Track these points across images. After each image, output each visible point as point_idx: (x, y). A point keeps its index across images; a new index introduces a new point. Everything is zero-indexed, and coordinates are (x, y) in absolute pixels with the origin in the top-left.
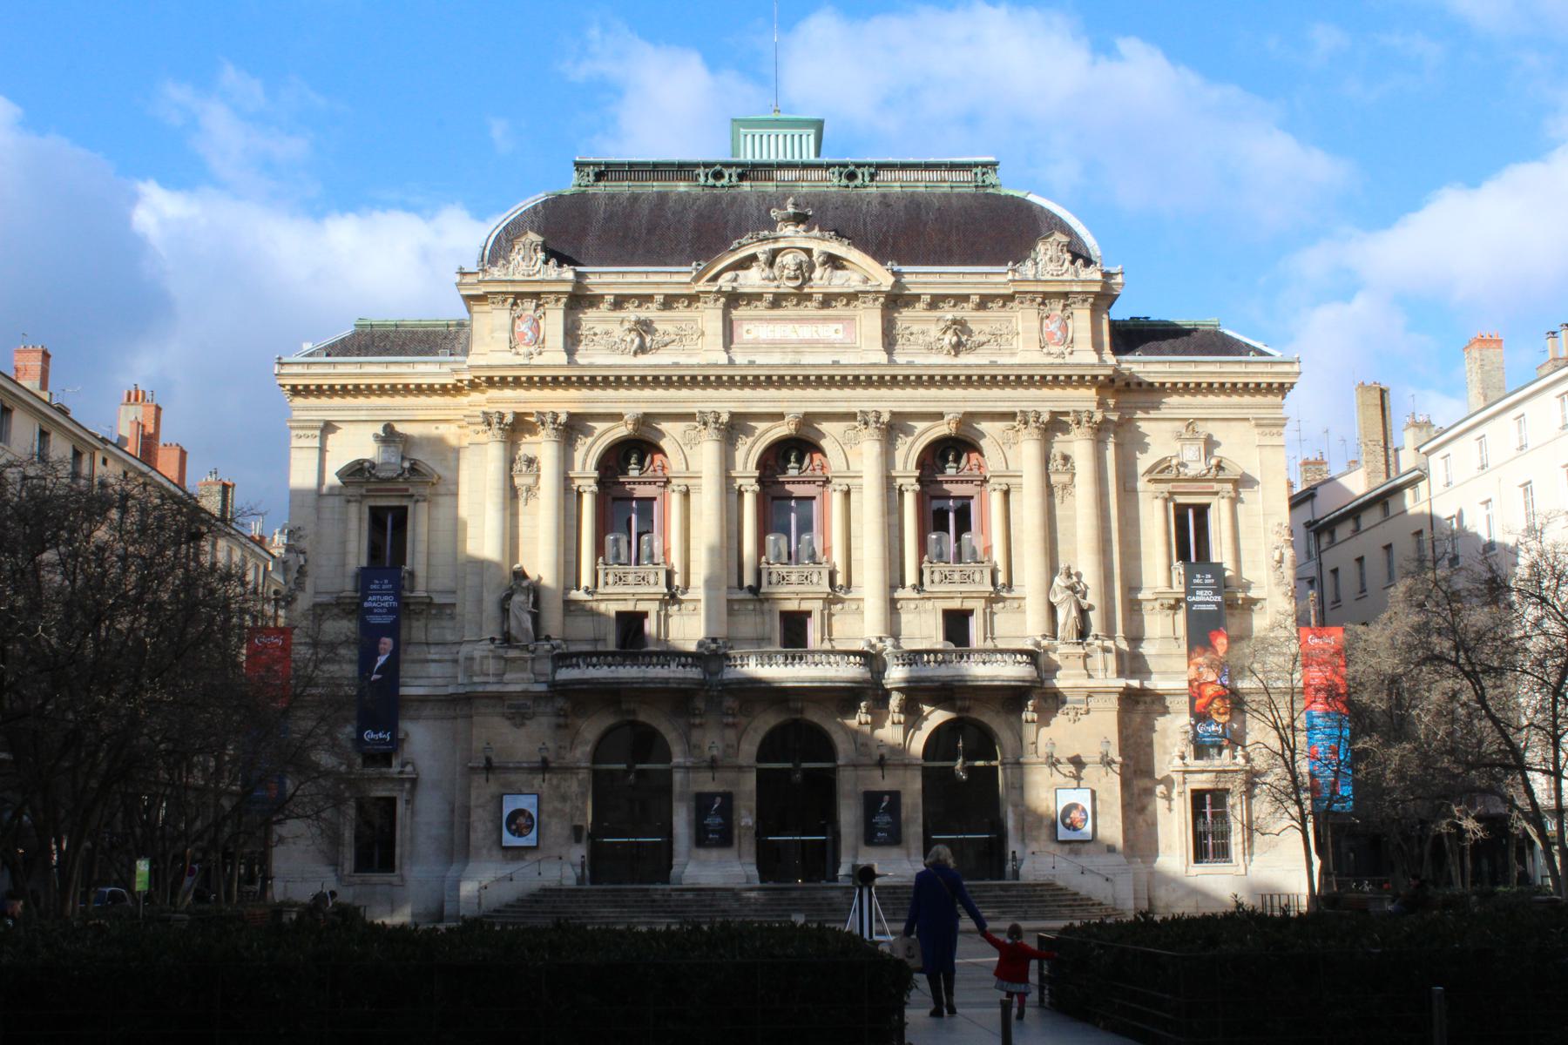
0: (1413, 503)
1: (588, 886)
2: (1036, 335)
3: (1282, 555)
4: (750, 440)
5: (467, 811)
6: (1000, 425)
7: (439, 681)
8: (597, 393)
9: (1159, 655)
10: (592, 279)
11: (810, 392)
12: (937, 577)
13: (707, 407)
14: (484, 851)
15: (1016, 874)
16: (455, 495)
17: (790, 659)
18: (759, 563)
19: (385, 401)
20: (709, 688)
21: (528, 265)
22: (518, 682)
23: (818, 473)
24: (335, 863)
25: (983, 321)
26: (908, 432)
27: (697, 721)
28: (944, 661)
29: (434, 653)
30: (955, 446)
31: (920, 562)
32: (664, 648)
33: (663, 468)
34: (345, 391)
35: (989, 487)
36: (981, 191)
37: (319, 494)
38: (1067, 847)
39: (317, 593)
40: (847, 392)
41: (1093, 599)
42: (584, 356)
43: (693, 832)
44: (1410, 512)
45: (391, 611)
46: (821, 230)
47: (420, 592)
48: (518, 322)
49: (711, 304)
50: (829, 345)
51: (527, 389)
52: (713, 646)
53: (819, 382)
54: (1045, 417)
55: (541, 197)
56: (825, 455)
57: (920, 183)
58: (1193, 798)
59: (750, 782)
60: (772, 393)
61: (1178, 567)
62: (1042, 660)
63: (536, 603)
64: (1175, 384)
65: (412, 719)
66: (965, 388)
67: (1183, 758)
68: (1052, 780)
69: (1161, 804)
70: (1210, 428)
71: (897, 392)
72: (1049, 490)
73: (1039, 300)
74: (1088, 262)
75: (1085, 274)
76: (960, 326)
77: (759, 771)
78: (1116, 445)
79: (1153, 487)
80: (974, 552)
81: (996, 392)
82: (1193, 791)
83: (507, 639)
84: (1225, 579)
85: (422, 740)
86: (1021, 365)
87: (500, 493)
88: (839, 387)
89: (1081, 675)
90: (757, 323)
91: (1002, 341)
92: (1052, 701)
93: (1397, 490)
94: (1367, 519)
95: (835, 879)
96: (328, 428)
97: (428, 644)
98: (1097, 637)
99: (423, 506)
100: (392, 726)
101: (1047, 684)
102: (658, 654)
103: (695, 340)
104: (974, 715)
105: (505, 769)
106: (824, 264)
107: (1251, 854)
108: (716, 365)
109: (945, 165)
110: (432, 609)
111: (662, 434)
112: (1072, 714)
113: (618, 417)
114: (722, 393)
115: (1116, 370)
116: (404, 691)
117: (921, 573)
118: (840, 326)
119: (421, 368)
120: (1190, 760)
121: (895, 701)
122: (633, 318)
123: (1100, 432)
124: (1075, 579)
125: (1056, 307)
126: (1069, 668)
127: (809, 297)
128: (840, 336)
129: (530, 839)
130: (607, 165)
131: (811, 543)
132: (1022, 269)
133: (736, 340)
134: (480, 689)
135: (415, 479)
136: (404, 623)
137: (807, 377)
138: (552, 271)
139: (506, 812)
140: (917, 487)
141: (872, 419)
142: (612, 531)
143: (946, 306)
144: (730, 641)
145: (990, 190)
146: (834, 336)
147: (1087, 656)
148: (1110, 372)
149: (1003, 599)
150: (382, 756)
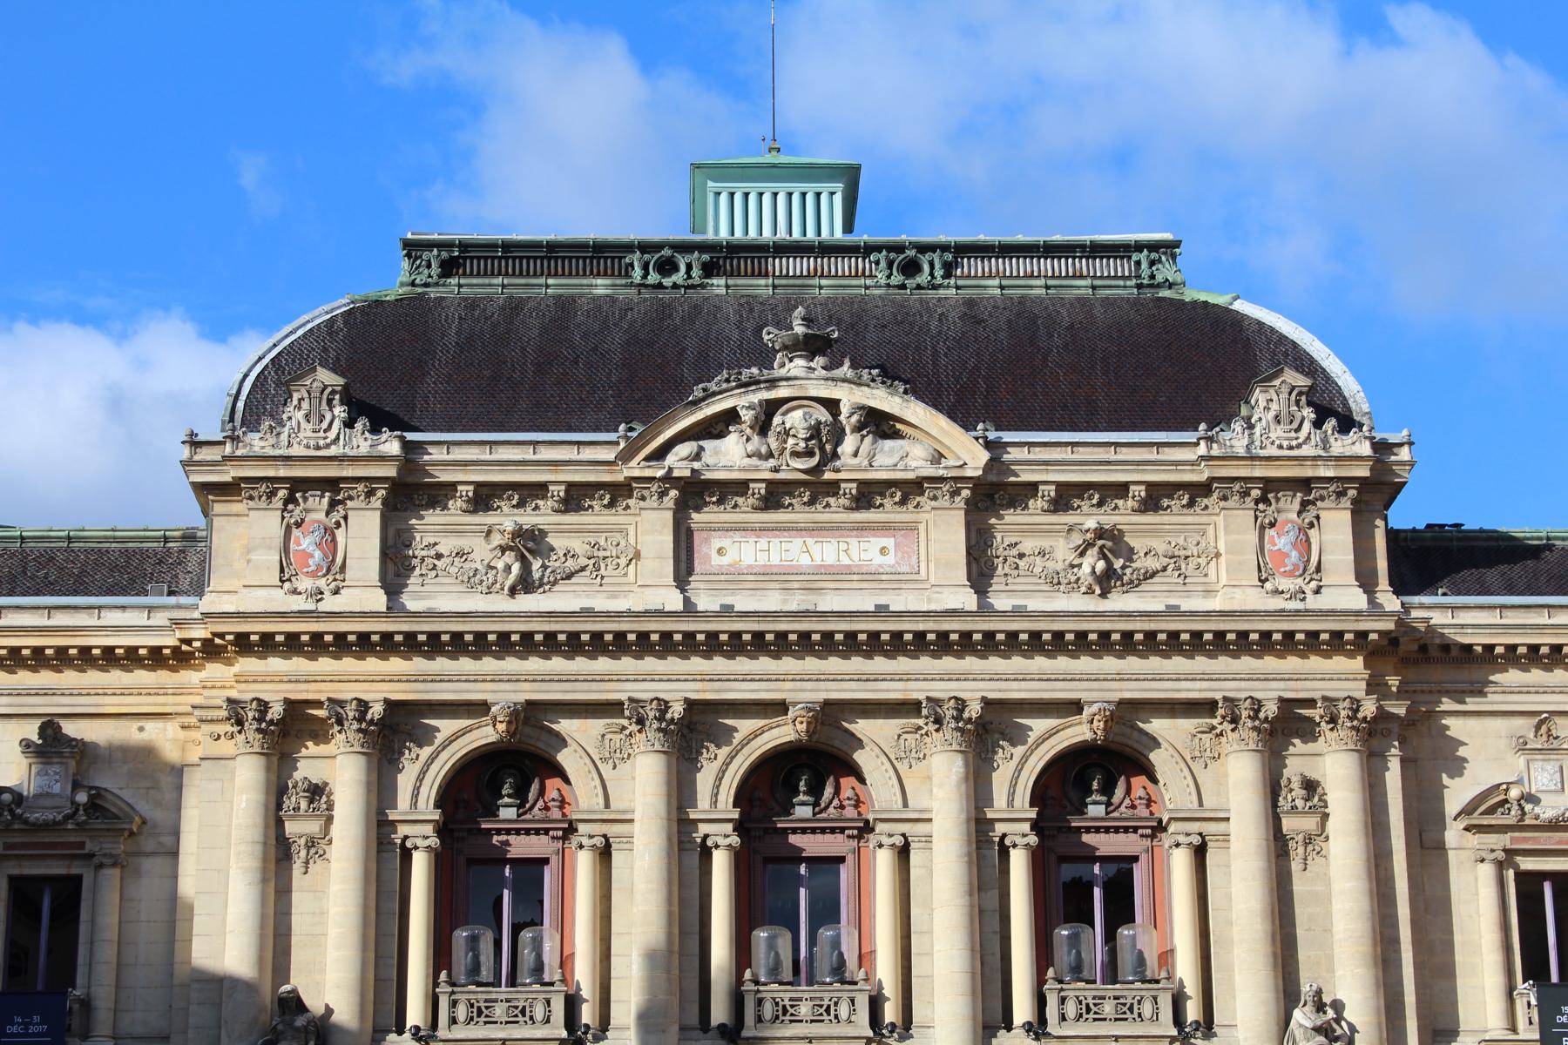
4: (724, 752)
6: (1187, 725)
8: (442, 664)
11: (834, 664)
12: (1071, 1009)
13: (644, 691)
16: (174, 854)
18: (739, 981)
19: (46, 678)
21: (312, 431)
23: (850, 812)
25: (1153, 531)
26: (1017, 736)
31: (1040, 981)
33: (563, 803)
35: (1166, 840)
36: (1148, 293)
40: (903, 664)
42: (417, 596)
46: (853, 366)
48: (296, 532)
49: (652, 502)
50: (870, 576)
51: (312, 657)
53: (851, 645)
55: (341, 304)
57: (1035, 280)
60: (765, 664)
61: (1527, 994)
64: (1512, 648)
66: (1120, 656)
71: (995, 663)
72: (1279, 846)
73: (1256, 493)
74: (1347, 424)
76: (1110, 541)
78: (1403, 761)
79: (1474, 840)
80: (1141, 960)
86: (1222, 614)
87: (258, 849)
90: (737, 536)
91: (1189, 568)
99: (112, 876)
103: (626, 567)
106: (858, 428)
108: (661, 614)
111: (561, 742)
113: (478, 709)
114: (673, 664)
115: (1400, 623)
118: (889, 542)
119: (112, 618)
122: (509, 526)
123: (1373, 738)
124: (1331, 1014)
125: (1289, 506)
127: (833, 488)
128: (890, 559)
130: (464, 246)
131: (836, 943)
132: (1226, 435)
135: (98, 824)
137: (828, 636)
138: (361, 441)
140: (1033, 840)
141: (949, 712)
142: (464, 923)
143: (1085, 505)
145: (1165, 293)
146: (879, 560)
148: (1390, 626)
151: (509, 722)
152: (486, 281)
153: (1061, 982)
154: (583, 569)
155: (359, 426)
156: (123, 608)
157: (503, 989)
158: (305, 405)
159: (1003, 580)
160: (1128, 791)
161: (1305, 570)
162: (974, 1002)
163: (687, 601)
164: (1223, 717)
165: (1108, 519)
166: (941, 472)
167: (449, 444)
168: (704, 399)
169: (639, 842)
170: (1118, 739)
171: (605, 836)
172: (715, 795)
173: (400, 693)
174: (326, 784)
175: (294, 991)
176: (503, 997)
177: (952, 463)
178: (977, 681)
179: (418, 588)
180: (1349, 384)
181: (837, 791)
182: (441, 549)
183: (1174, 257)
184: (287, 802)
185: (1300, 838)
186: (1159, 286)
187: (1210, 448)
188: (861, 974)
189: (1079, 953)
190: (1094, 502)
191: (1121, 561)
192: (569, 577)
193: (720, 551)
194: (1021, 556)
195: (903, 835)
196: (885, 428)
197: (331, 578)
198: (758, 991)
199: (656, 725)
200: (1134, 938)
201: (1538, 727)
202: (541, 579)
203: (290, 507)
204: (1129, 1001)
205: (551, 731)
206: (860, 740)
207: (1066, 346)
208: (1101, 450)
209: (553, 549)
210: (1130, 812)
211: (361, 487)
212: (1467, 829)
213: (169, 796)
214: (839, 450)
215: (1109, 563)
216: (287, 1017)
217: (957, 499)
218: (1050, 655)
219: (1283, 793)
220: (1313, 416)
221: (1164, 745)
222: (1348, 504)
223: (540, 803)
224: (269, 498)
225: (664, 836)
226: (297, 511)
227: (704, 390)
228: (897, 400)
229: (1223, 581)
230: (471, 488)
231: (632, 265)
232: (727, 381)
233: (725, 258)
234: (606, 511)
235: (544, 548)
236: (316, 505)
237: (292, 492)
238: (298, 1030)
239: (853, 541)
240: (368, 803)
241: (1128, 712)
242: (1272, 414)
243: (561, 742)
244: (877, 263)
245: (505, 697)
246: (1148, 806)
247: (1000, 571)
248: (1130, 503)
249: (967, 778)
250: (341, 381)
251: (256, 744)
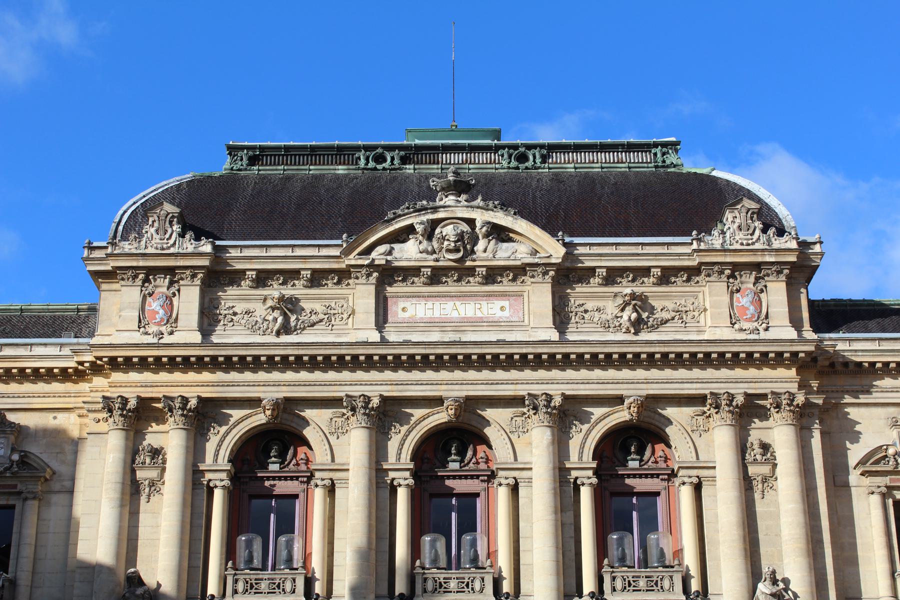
4: (404, 429)
8: (234, 376)
11: (472, 374)
12: (619, 584)
13: (356, 391)
16: (71, 492)
18: (413, 567)
21: (161, 240)
23: (483, 466)
25: (666, 296)
26: (584, 418)
33: (307, 461)
35: (677, 481)
36: (662, 170)
40: (514, 374)
48: (149, 299)
49: (363, 280)
50: (495, 324)
51: (156, 372)
53: (482, 362)
54: (740, 400)
55: (188, 176)
60: (430, 375)
64: (886, 364)
71: (570, 374)
72: (747, 484)
73: (727, 272)
75: (778, 243)
76: (640, 302)
78: (822, 433)
79: (867, 481)
80: (662, 554)
87: (119, 486)
90: (414, 300)
99: (33, 505)
106: (486, 236)
108: (366, 344)
109: (623, 145)
111: (306, 423)
113: (254, 403)
114: (374, 375)
115: (817, 347)
118: (506, 303)
122: (276, 294)
123: (803, 418)
124: (781, 585)
125: (748, 280)
127: (471, 271)
128: (506, 313)
130: (262, 148)
131: (474, 543)
133: (390, 319)
135: (25, 473)
137: (468, 357)
138: (189, 245)
140: (594, 480)
141: (542, 402)
143: (624, 281)
145: (672, 170)
146: (499, 314)
148: (812, 348)
151: (273, 410)
152: (275, 167)
153: (612, 567)
154: (321, 321)
155: (188, 236)
156: (45, 345)
157: (269, 572)
158: (156, 224)
159: (575, 325)
160: (653, 453)
161: (758, 318)
162: (558, 579)
163: (382, 337)
164: (711, 405)
166: (536, 261)
167: (242, 247)
168: (394, 219)
169: (351, 483)
170: (646, 420)
171: (331, 479)
172: (399, 454)
173: (207, 393)
174: (163, 448)
175: (136, 572)
176: (266, 577)
177: (543, 255)
179: (222, 332)
180: (782, 211)
181: (475, 453)
182: (236, 310)
183: (677, 151)
184: (138, 459)
185: (759, 479)
186: (668, 167)
187: (699, 245)
188: (489, 562)
189: (623, 550)
190: (630, 279)
191: (647, 314)
193: (404, 309)
194: (586, 311)
195: (515, 478)
196: (503, 236)
197: (169, 325)
198: (424, 573)
199: (362, 411)
200: (658, 539)
202: (296, 326)
203: (146, 284)
204: (655, 579)
205: (299, 416)
206: (488, 421)
207: (612, 193)
208: (633, 247)
209: (303, 309)
210: (654, 465)
211: (188, 272)
212: (862, 474)
213: (70, 457)
214: (475, 248)
215: (639, 315)
216: (132, 589)
217: (547, 277)
218: (604, 368)
219: (749, 451)
220: (761, 226)
221: (675, 423)
222: (784, 278)
223: (294, 461)
224: (133, 279)
225: (367, 478)
226: (150, 287)
227: (394, 214)
228: (510, 218)
229: (709, 323)
230: (254, 273)
231: (359, 158)
232: (408, 208)
233: (414, 154)
234: (336, 287)
235: (298, 308)
236: (161, 283)
237: (147, 276)
238: (138, 596)
239: (484, 303)
240: (187, 459)
241: (651, 403)
242: (736, 225)
243: (306, 423)
244: (502, 156)
245: (269, 395)
246: (665, 462)
247: (573, 320)
248: (652, 279)
249: (553, 442)
250: (178, 210)
251: (120, 424)
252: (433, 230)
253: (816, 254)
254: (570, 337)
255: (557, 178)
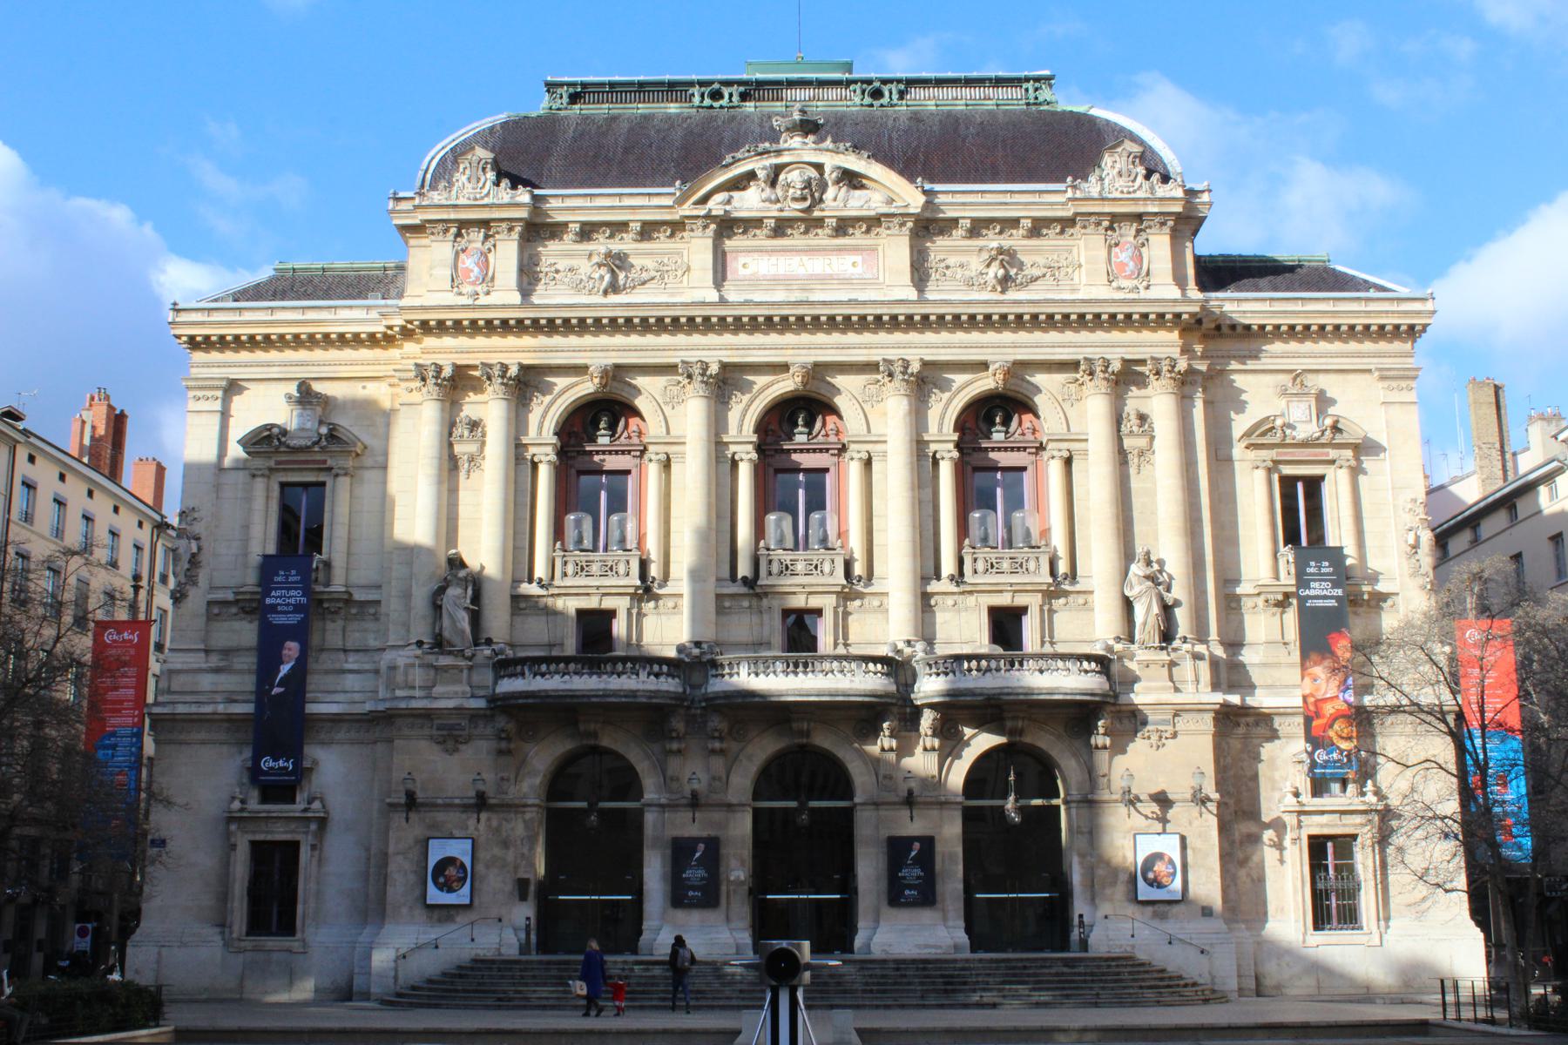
0: (1548, 502)
1: (534, 957)
2: (1103, 267)
3: (1417, 538)
4: (746, 398)
5: (384, 858)
6: (1060, 378)
7: (357, 697)
8: (557, 340)
9: (1265, 665)
10: (554, 203)
12: (980, 566)
13: (692, 356)
14: (404, 911)
15: (1084, 945)
16: (384, 467)
17: (795, 667)
18: (757, 548)
19: (302, 355)
20: (692, 704)
21: (475, 189)
22: (451, 696)
23: (833, 438)
24: (223, 925)
25: (1037, 251)
26: (944, 386)
27: (675, 746)
28: (989, 670)
29: (352, 662)
30: (1003, 406)
32: (636, 653)
33: (640, 434)
34: (252, 343)
35: (1045, 455)
37: (219, 468)
38: (1150, 909)
39: (212, 588)
40: (867, 337)
41: (1179, 592)
43: (669, 888)
44: (1546, 512)
45: (298, 608)
46: (834, 142)
47: (338, 585)
48: (462, 256)
49: (699, 233)
50: (846, 281)
51: (472, 336)
52: (696, 651)
53: (832, 324)
54: (1116, 366)
55: (502, 117)
56: (840, 417)
57: (958, 100)
58: (1311, 847)
59: (742, 826)
61: (1287, 554)
62: (1115, 668)
63: (476, 599)
64: (1277, 327)
65: (323, 743)
66: (1015, 331)
67: (1297, 795)
68: (1130, 823)
69: (1270, 855)
70: (1323, 382)
71: (929, 337)
73: (1106, 224)
74: (1166, 179)
75: (1162, 191)
76: (1007, 257)
77: (757, 813)
78: (1206, 403)
79: (1252, 454)
80: (1028, 534)
81: (1053, 336)
82: (1311, 837)
83: (439, 644)
84: (1347, 568)
85: (333, 770)
86: (1083, 301)
87: (436, 462)
88: (857, 331)
89: (1164, 689)
90: (756, 255)
91: (1061, 275)
92: (1131, 721)
93: (1529, 488)
94: (1488, 527)
95: (851, 951)
96: (232, 388)
97: (345, 651)
98: (1185, 640)
99: (344, 482)
100: (296, 753)
101: (1123, 700)
102: (624, 660)
103: (681, 274)
104: (1027, 739)
105: (431, 806)
106: (838, 182)
107: (1387, 919)
108: (703, 304)
109: (990, 80)
110: (350, 606)
111: (638, 391)
112: (1154, 738)
113: (580, 370)
114: (712, 339)
115: (1203, 308)
116: (311, 708)
117: (961, 562)
118: (858, 258)
119: (344, 314)
120: (1306, 798)
121: (927, 720)
122: (603, 249)
123: (1185, 383)
125: (1128, 231)
126: (1149, 680)
127: (819, 223)
128: (858, 270)
129: (462, 896)
130: (584, 85)
131: (823, 523)
132: (1084, 185)
133: (729, 276)
134: (403, 705)
135: (334, 448)
136: (316, 625)
137: (816, 318)
138: (504, 194)
139: (432, 861)
140: (956, 454)
141: (898, 369)
142: (576, 510)
143: (991, 233)
144: (720, 645)
146: (851, 271)
147: (1172, 664)
148: (1196, 309)
149: (1066, 594)
150: (279, 790)
156: (351, 307)
160: (1020, 424)
163: (721, 297)
165: (1006, 243)
166: (892, 210)
167: (563, 196)
173: (530, 359)
178: (918, 347)
181: (824, 425)
182: (558, 267)
192: (644, 283)
193: (744, 265)
194: (948, 267)
201: (1295, 379)
205: (630, 385)
211: (504, 225)
218: (967, 330)
228: (863, 163)
229: (1084, 281)
237: (459, 229)
240: (508, 431)
241: (1019, 369)
243: (638, 391)
248: (1021, 232)
249: (910, 412)
250: (492, 155)
252: (777, 176)
253: (1204, 204)
254: (930, 296)
255: (916, 118)
